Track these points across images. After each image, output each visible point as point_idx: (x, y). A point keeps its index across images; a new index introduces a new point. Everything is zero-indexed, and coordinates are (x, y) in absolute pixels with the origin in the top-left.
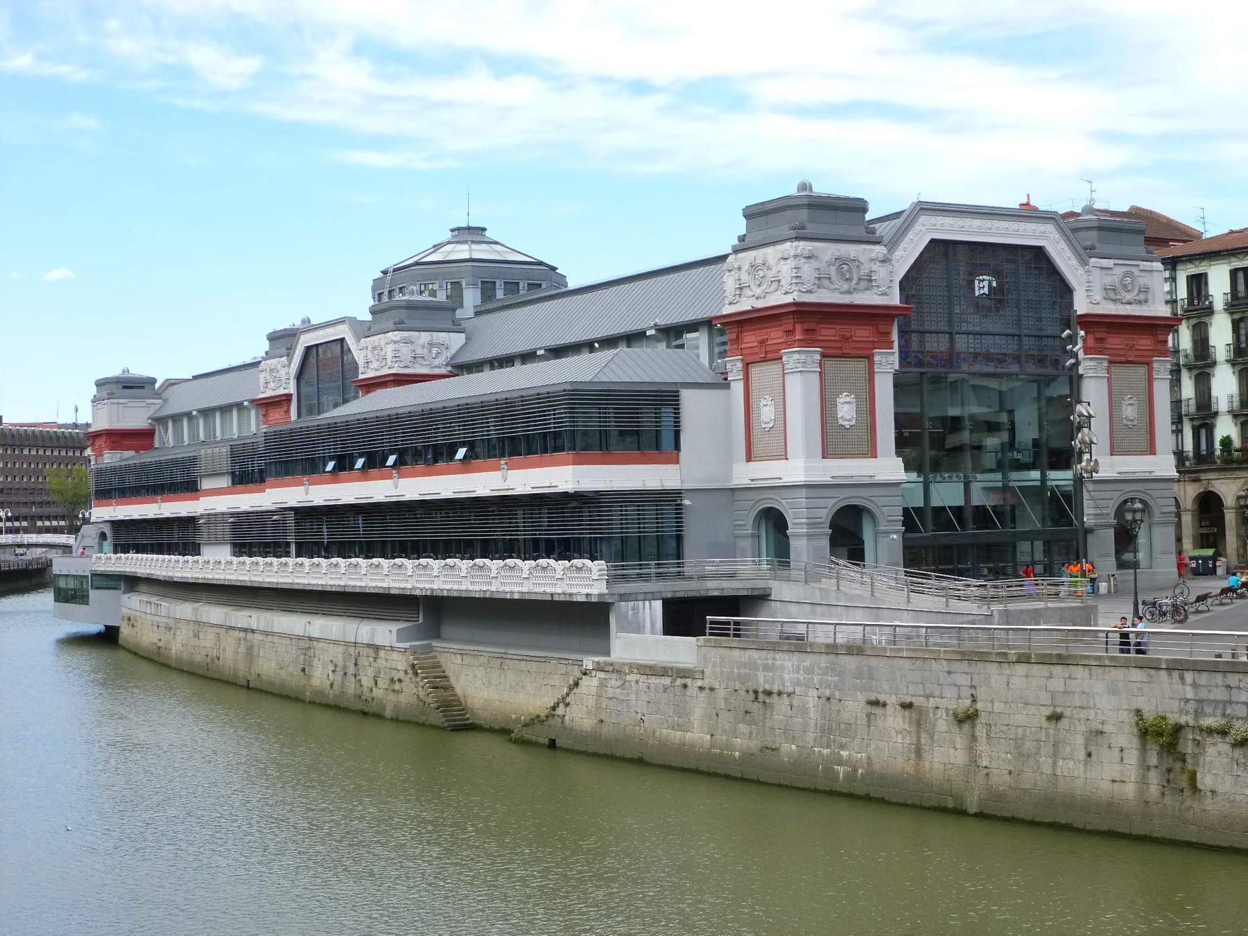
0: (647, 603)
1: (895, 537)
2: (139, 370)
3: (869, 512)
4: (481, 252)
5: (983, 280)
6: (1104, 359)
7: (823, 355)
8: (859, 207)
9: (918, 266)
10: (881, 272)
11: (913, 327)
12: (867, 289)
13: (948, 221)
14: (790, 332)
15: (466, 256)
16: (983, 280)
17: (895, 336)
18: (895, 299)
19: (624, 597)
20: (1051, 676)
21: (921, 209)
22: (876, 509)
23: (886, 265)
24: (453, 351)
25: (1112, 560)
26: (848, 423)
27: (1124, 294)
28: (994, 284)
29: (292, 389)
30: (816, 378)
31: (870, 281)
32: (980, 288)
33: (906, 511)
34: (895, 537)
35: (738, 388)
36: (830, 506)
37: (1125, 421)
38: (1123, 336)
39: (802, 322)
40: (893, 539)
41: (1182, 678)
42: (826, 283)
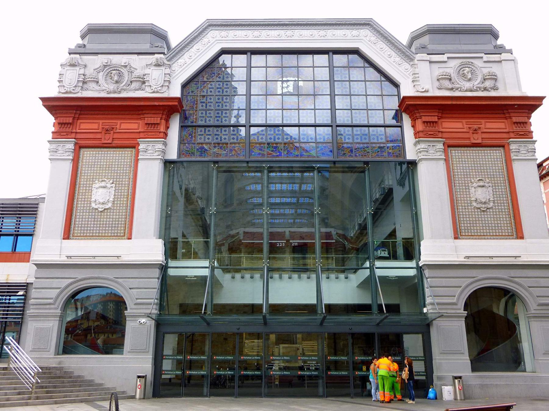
6: (440, 141)
25: (465, 360)
26: (101, 206)
27: (464, 83)
32: (282, 88)
37: (474, 204)
38: (464, 121)
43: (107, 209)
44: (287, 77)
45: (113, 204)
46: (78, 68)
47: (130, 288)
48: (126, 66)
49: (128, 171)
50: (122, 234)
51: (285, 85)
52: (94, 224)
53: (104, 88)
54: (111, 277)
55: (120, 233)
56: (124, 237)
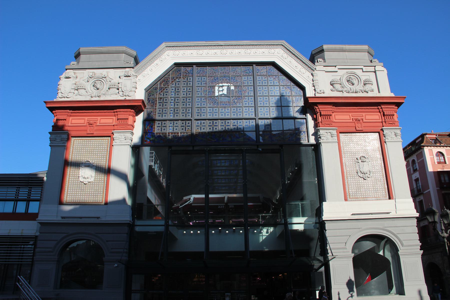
5: (222, 86)
16: (222, 86)
28: (232, 88)
32: (219, 91)
44: (222, 83)
49: (105, 154)
51: (221, 89)
52: (81, 194)
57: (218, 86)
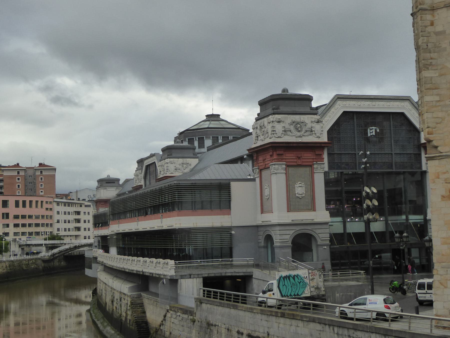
0: (195, 279)
1: (325, 247)
2: (114, 175)
3: (314, 236)
4: (214, 124)
7: (287, 166)
8: (309, 99)
9: (337, 123)
10: (317, 127)
11: (336, 152)
12: (310, 135)
13: (352, 103)
14: (271, 156)
15: (206, 126)
16: (372, 129)
17: (325, 156)
18: (324, 139)
19: (182, 277)
20: (291, 325)
21: (338, 98)
22: (316, 234)
23: (319, 124)
24: (193, 166)
26: (301, 196)
28: (378, 131)
29: (142, 183)
30: (284, 176)
31: (312, 131)
32: (370, 133)
33: (330, 234)
34: (325, 247)
35: (258, 180)
36: (291, 233)
39: (276, 151)
40: (325, 249)
41: (333, 329)
42: (289, 133)
43: (303, 197)
44: (372, 127)
45: (305, 194)
46: (281, 123)
47: (318, 233)
48: (303, 122)
50: (311, 209)
51: (371, 131)
52: (298, 204)
53: (294, 134)
54: (310, 229)
55: (310, 208)
56: (312, 210)
57: (369, 129)
